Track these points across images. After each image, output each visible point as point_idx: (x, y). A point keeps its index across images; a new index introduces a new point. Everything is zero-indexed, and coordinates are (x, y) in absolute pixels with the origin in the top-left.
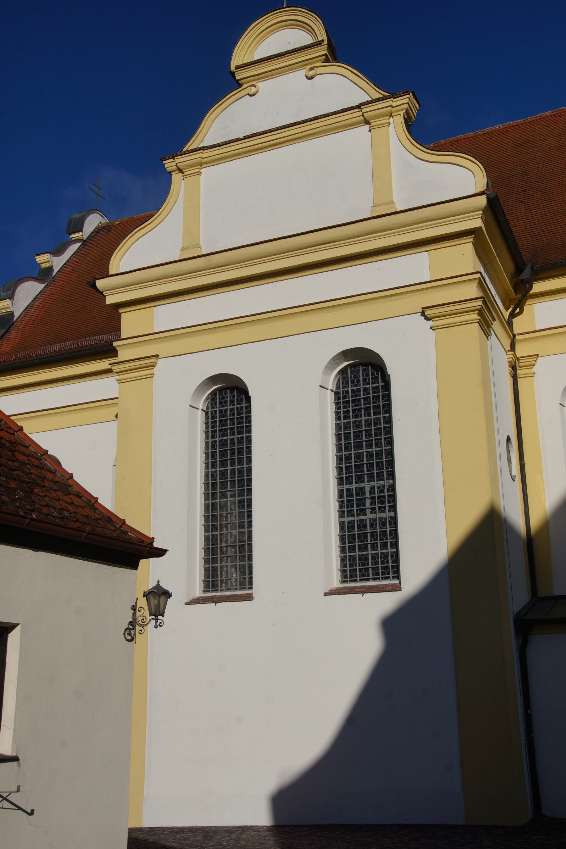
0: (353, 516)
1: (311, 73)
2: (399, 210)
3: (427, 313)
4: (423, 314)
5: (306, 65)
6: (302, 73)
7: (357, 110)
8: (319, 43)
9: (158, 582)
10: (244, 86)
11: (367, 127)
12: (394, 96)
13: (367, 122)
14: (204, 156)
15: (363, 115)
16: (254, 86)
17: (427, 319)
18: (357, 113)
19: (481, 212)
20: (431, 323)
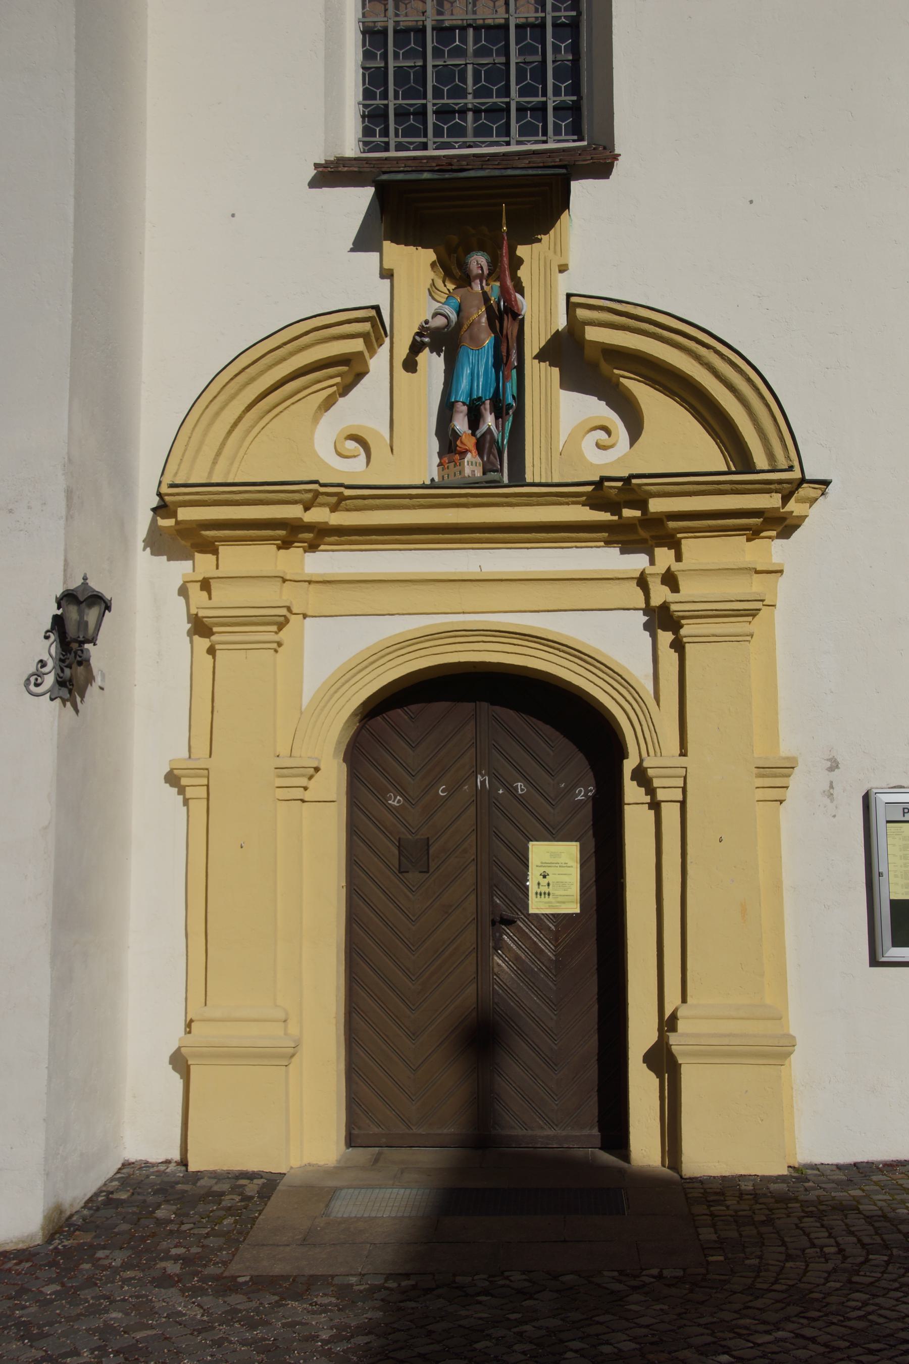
9: (85, 578)
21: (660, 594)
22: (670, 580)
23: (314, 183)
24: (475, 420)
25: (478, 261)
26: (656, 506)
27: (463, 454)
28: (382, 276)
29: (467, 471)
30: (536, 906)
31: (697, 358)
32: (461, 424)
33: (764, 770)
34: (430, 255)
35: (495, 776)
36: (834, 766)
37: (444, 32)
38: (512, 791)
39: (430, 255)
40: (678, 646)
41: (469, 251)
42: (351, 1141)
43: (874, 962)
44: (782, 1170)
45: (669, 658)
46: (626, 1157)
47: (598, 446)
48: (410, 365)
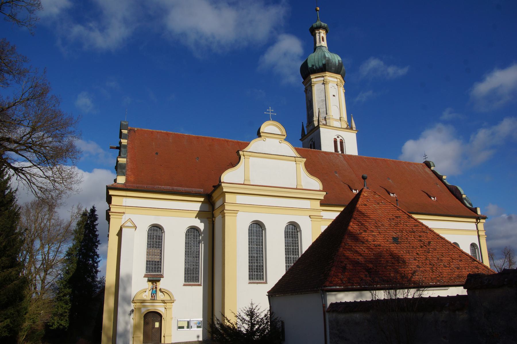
0: (291, 264)
1: (281, 142)
2: (304, 188)
3: (311, 217)
4: (310, 216)
6: (278, 140)
8: (285, 135)
12: (303, 158)
13: (295, 161)
14: (252, 154)
16: (265, 139)
17: (310, 218)
18: (294, 158)
20: (311, 219)
21: (165, 307)
23: (144, 277)
24: (154, 294)
25: (154, 283)
26: (165, 302)
30: (156, 327)
32: (153, 295)
33: (171, 318)
34: (151, 283)
35: (153, 318)
37: (152, 261)
39: (151, 283)
42: (143, 343)
44: (170, 343)
48: (150, 291)
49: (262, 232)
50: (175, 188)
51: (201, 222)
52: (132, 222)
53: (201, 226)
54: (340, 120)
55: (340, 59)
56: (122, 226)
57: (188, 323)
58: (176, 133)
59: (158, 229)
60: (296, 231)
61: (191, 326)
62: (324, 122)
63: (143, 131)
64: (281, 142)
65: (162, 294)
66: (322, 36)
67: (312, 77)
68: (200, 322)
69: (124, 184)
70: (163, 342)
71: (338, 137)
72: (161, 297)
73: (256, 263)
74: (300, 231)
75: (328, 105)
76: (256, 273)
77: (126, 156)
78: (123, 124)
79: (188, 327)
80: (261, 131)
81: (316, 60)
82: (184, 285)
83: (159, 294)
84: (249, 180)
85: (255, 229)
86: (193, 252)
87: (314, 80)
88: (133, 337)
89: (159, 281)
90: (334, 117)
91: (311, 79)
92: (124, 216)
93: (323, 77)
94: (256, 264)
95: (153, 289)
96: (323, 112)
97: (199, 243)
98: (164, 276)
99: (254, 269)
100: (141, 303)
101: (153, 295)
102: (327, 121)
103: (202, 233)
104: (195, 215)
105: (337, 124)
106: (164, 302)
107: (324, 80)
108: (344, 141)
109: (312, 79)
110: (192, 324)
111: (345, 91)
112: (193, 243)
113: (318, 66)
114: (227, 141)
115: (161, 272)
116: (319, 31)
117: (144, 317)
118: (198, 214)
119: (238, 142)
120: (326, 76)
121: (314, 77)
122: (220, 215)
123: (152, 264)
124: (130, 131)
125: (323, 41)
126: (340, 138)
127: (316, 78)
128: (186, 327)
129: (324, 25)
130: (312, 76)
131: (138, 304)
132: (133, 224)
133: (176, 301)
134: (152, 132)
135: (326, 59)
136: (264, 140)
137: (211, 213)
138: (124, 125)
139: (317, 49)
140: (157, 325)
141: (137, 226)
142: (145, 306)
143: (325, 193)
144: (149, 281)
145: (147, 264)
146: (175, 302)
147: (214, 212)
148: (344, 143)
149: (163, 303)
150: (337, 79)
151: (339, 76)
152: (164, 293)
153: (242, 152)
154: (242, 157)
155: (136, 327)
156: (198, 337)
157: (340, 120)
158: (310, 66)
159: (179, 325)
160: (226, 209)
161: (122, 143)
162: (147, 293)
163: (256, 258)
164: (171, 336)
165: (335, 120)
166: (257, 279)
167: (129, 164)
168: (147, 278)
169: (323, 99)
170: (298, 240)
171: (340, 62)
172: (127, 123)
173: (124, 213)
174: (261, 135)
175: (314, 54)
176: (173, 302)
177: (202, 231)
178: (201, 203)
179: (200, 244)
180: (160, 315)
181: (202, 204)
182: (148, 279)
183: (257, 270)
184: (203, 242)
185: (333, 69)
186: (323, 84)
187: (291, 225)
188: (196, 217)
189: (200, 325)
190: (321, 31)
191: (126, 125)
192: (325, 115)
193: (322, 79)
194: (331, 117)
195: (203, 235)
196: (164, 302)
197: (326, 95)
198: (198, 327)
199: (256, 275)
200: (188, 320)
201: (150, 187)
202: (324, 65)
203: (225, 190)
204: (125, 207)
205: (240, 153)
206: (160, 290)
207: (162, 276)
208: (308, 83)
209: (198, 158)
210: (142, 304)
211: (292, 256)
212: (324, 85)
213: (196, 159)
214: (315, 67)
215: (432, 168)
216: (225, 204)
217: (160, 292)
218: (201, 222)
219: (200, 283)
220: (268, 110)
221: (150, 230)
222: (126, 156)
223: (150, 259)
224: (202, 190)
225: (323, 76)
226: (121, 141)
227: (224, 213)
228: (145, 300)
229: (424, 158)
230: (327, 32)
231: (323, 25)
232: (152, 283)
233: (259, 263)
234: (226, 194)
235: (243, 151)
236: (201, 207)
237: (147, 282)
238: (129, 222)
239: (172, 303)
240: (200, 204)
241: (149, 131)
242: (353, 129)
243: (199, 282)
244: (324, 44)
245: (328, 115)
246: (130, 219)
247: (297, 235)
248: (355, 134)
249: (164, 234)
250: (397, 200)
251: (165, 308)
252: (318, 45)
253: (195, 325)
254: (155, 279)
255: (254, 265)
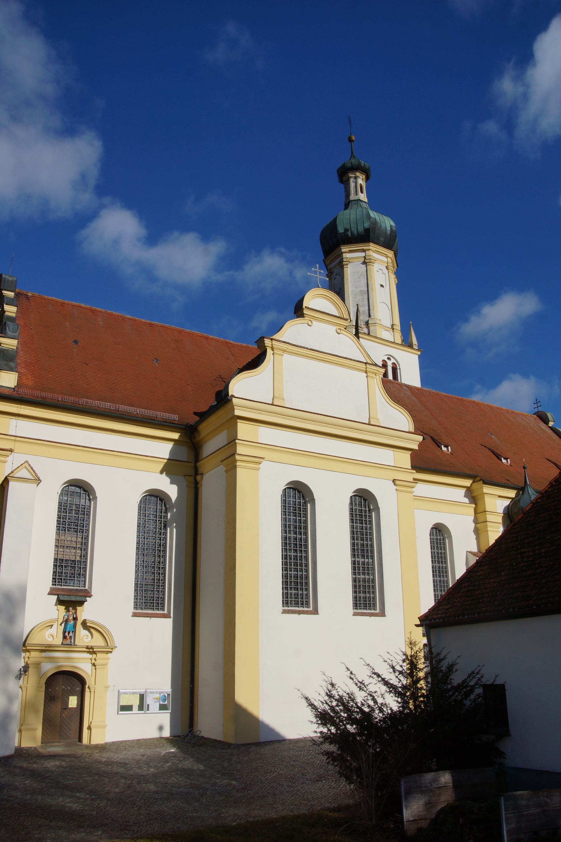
1: (339, 331)
3: (397, 482)
4: (394, 481)
5: (339, 326)
7: (364, 364)
10: (306, 318)
11: (365, 375)
13: (366, 372)
14: (289, 348)
15: (366, 368)
16: (311, 322)
17: (395, 485)
18: (363, 366)
19: (419, 443)
21: (93, 661)
22: (95, 659)
23: (49, 594)
24: (69, 633)
25: (71, 609)
26: (95, 650)
27: (67, 639)
28: (57, 610)
29: (68, 642)
30: (70, 706)
31: (102, 629)
32: (67, 634)
33: (106, 687)
34: (64, 607)
35: (65, 686)
36: (114, 686)
38: (67, 689)
39: (64, 607)
40: (95, 669)
41: (71, 606)
43: (118, 714)
44: (103, 742)
45: (94, 670)
46: (82, 743)
47: (86, 638)
48: (61, 625)
49: (306, 506)
50: (123, 408)
51: (172, 483)
52: (32, 469)
53: (172, 491)
54: (393, 329)
55: (393, 224)
56: (8, 476)
57: (142, 697)
58: (108, 311)
59: (82, 492)
60: (367, 509)
61: (148, 705)
62: (366, 330)
63: (44, 299)
64: (339, 331)
65: (86, 632)
66: (361, 184)
67: (343, 250)
68: (165, 696)
69: (14, 389)
70: (85, 740)
71: (389, 359)
72: (86, 640)
73: (294, 571)
74: (377, 509)
75: (373, 301)
76: (293, 592)
77: (17, 334)
78: (5, 279)
79: (141, 708)
80: (305, 304)
81: (351, 220)
82: (135, 615)
83: (81, 633)
84: (283, 399)
85: (292, 500)
86: (153, 545)
87: (346, 256)
88: (20, 731)
89: (81, 603)
90: (382, 323)
91: (342, 253)
92: (11, 456)
93: (364, 251)
94: (293, 572)
95: (66, 621)
96: (364, 312)
97: (165, 527)
98: (93, 593)
99: (291, 582)
100: (42, 651)
101: (67, 634)
102: (371, 328)
103: (172, 506)
104: (161, 466)
105: (387, 335)
106: (91, 650)
107: (365, 257)
108: (398, 367)
109: (344, 254)
110: (149, 700)
111: (397, 282)
112: (153, 525)
113: (355, 232)
114: (207, 338)
115: (85, 584)
116: (355, 174)
117: (46, 683)
118: (166, 465)
119: (226, 342)
120: (369, 250)
121: (347, 250)
122: (222, 466)
123: (66, 566)
124: (18, 295)
125: (362, 192)
126: (393, 361)
127: (351, 252)
128: (135, 708)
129: (365, 164)
130: (344, 249)
131: (33, 654)
132: (34, 474)
133: (116, 649)
134: (63, 304)
135: (371, 219)
136: (310, 323)
137: (193, 465)
138: (8, 281)
139: (350, 205)
140: (73, 702)
141: (41, 478)
142: (51, 659)
143: (420, 438)
144: (60, 602)
145: (55, 566)
146: (115, 651)
147: (198, 464)
148: (398, 370)
149: (89, 652)
150: (387, 257)
151: (391, 254)
152: (92, 630)
153: (270, 341)
154: (269, 352)
155: (27, 707)
156: (161, 728)
157: (393, 329)
158: (341, 230)
159: (123, 703)
160: (238, 452)
161: (7, 313)
162: (53, 631)
163: (294, 559)
164: (104, 727)
165: (384, 327)
166: (296, 604)
167: (21, 353)
168: (56, 596)
169: (362, 289)
170: (371, 528)
171: (394, 229)
172: (15, 279)
173: (11, 451)
174: (304, 312)
175: (347, 211)
176: (111, 652)
177: (173, 500)
178: (173, 443)
179: (168, 529)
180: (81, 681)
181: (173, 445)
182: (58, 598)
183: (296, 586)
184: (175, 524)
185: (382, 239)
186: (364, 263)
187: (358, 496)
188: (161, 472)
189: (166, 703)
190: (358, 174)
191: (12, 281)
192: (367, 319)
193: (363, 254)
194: (377, 322)
195: (175, 510)
196: (91, 650)
197: (369, 284)
198: (163, 707)
199: (295, 595)
200: (142, 691)
201: (70, 399)
202: (367, 231)
203: (237, 412)
204: (14, 438)
205: (265, 342)
206: (84, 624)
207: (87, 594)
208: (336, 259)
209: (157, 360)
210: (44, 654)
211: (361, 560)
212: (366, 266)
213: (153, 361)
214: (349, 233)
215: (551, 424)
216: (237, 441)
217: (84, 629)
218: (172, 483)
219: (166, 612)
220: (313, 269)
221: (64, 492)
222: (17, 334)
223: (60, 557)
224: (175, 417)
225: (363, 249)
226: (5, 307)
227: (236, 461)
228: (50, 646)
229: (536, 406)
230: (367, 179)
231: (363, 165)
232: (65, 609)
233: (300, 571)
234: (238, 421)
235: (272, 339)
236: (172, 452)
237: (56, 605)
238: (25, 470)
239: (107, 652)
240: (170, 445)
241: (57, 301)
242: (414, 347)
243: (163, 610)
244: (363, 197)
245: (372, 317)
246: (27, 462)
247: (370, 517)
248: (417, 357)
249: (95, 504)
250: (524, 468)
251: (94, 665)
252: (352, 197)
253: (155, 702)
254: (73, 598)
255: (290, 574)
